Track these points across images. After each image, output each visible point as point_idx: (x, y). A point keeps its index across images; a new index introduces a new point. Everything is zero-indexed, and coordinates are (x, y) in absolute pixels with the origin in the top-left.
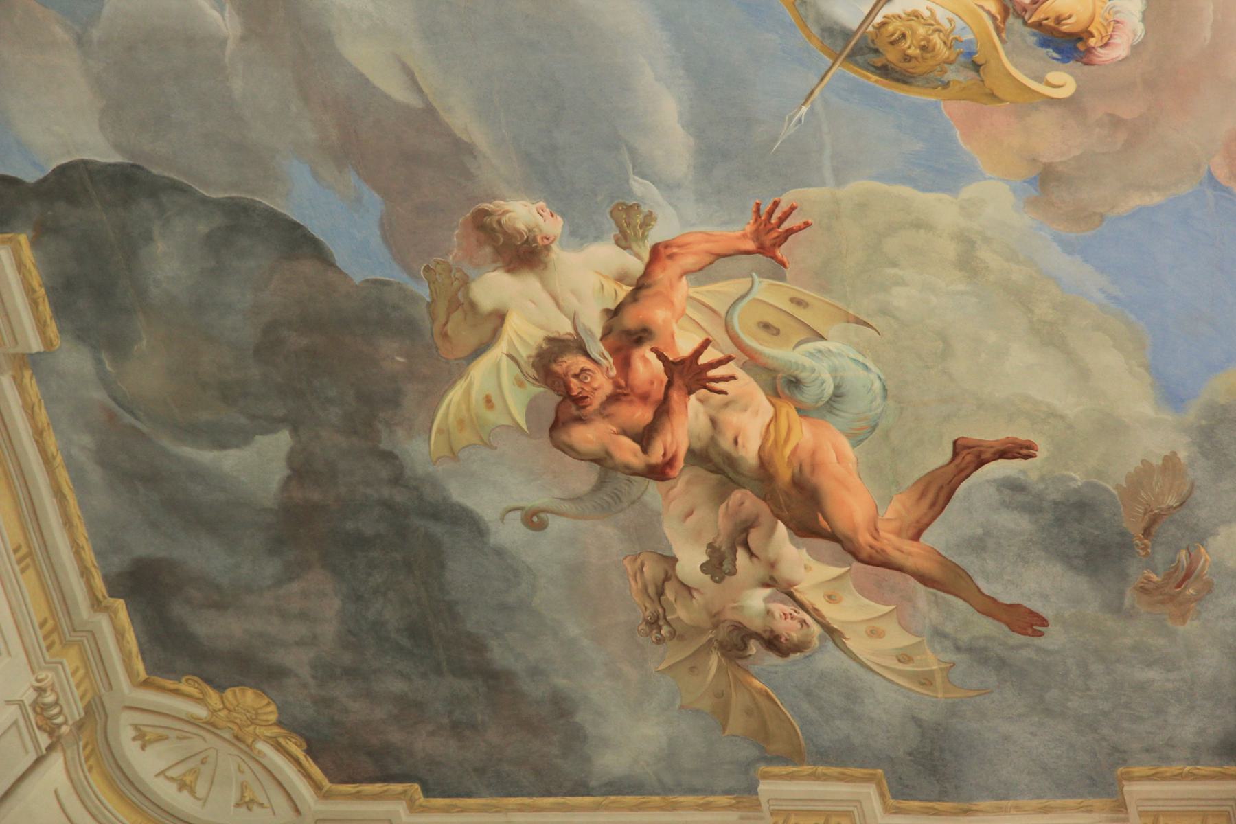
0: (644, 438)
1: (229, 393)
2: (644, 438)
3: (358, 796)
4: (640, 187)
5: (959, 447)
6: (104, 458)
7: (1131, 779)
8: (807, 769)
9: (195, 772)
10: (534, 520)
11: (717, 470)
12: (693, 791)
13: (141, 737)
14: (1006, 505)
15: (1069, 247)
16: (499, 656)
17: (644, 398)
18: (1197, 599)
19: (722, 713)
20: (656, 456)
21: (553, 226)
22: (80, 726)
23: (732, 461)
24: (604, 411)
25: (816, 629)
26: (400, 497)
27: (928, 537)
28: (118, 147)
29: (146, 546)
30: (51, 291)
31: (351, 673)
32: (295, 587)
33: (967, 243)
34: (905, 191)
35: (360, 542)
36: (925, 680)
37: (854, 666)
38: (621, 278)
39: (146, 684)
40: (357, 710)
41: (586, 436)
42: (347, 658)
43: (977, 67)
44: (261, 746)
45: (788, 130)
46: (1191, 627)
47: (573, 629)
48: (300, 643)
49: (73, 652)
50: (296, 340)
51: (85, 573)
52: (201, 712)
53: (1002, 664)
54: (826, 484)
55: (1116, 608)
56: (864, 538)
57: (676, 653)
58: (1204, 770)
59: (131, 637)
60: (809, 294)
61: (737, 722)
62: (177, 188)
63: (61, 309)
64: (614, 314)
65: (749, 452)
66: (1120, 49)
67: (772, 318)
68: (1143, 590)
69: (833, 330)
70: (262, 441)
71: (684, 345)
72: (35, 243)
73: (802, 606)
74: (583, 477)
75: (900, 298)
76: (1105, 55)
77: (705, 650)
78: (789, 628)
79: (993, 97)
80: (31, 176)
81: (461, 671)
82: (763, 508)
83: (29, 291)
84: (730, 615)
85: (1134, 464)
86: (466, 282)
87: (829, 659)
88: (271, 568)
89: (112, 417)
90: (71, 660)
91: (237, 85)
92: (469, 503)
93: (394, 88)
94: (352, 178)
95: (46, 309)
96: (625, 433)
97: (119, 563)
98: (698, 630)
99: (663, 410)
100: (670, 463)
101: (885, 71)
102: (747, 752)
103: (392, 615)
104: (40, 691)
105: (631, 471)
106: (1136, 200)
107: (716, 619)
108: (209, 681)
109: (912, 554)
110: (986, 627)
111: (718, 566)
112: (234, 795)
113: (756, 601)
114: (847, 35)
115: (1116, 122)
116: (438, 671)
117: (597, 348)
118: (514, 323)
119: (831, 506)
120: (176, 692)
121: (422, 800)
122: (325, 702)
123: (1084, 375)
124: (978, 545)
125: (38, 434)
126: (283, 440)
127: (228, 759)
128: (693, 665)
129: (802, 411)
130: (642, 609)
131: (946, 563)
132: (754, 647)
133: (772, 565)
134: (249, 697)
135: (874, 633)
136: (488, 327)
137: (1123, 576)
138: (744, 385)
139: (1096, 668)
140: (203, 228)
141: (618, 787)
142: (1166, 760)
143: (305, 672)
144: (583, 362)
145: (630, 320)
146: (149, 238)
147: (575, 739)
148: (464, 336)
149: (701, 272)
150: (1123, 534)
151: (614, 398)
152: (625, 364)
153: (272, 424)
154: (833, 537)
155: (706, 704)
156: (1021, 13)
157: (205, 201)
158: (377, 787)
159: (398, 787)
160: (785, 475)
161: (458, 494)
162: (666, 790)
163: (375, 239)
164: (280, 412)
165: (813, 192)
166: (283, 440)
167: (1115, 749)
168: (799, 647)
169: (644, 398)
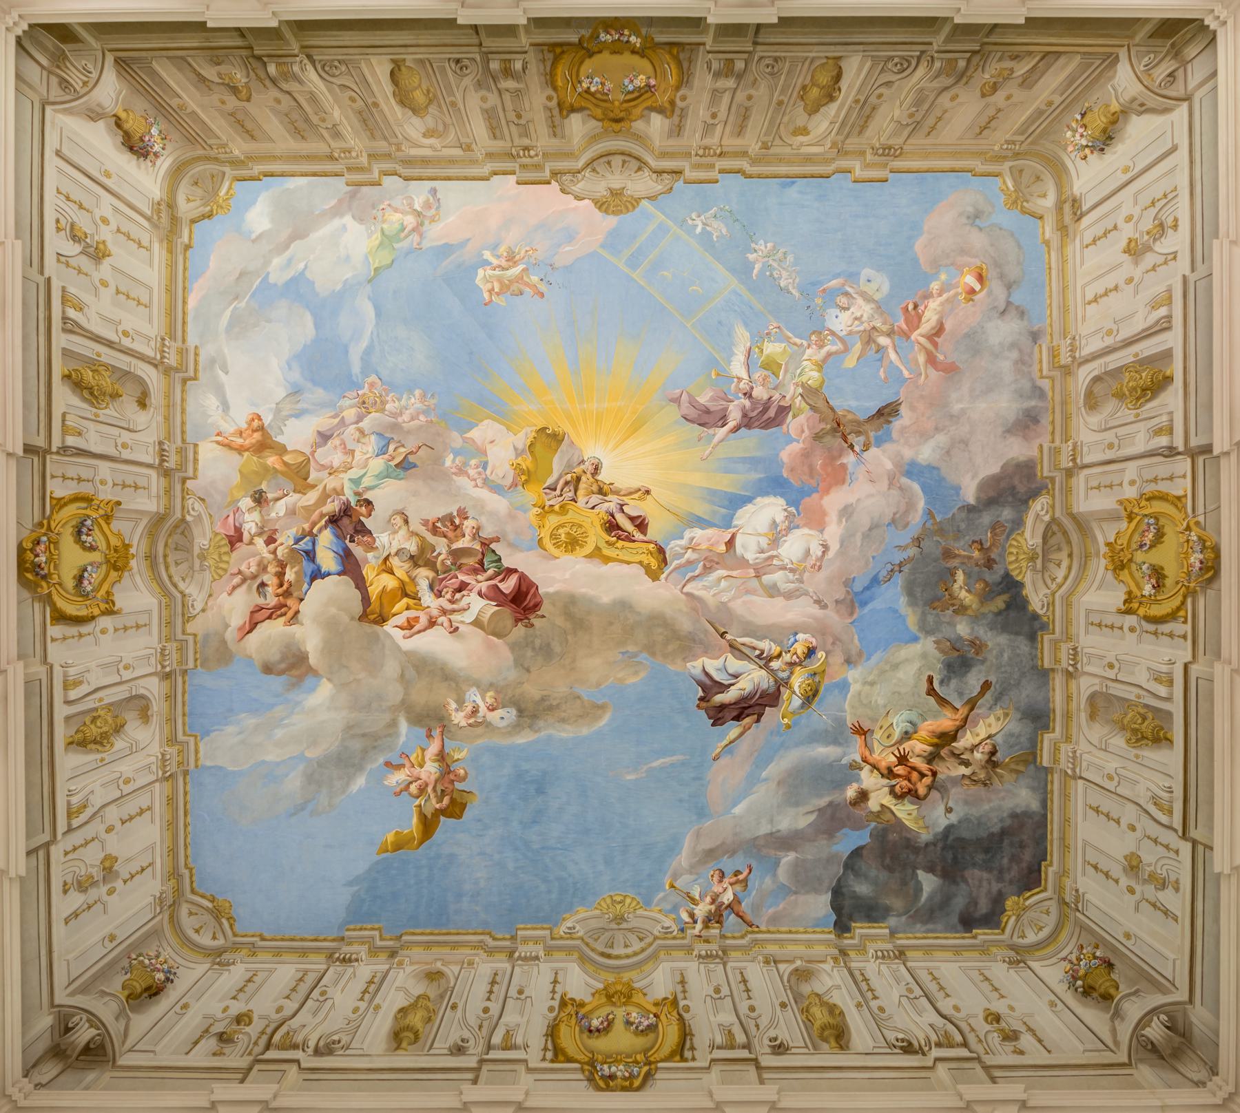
0: (923, 775)
1: (904, 883)
2: (923, 775)
3: (1046, 880)
4: (844, 761)
5: (928, 694)
6: (925, 923)
7: (1043, 665)
8: (1038, 752)
9: (1036, 925)
10: (949, 810)
11: (934, 758)
12: (1046, 785)
13: (1023, 937)
14: (948, 685)
15: (869, 659)
16: (996, 829)
17: (909, 773)
18: (980, 641)
19: (1018, 772)
20: (929, 773)
21: (855, 786)
22: (1017, 953)
23: (931, 754)
24: (914, 784)
25: (988, 741)
26: (940, 845)
27: (958, 706)
28: (827, 892)
29: (955, 919)
30: (869, 922)
31: (1001, 871)
32: (970, 881)
33: (865, 683)
34: (849, 696)
35: (955, 858)
36: (1006, 715)
37: (1002, 732)
38: (872, 772)
39: (1003, 931)
40: (1014, 872)
41: (922, 790)
42: (995, 872)
43: (815, 674)
44: (1027, 903)
45: (829, 721)
46: (990, 644)
47: (986, 807)
48: (990, 884)
49: (991, 949)
50: (888, 861)
51: (963, 938)
52: (1013, 918)
53: (1001, 693)
54: (940, 730)
55: (983, 662)
56: (958, 723)
57: (996, 780)
58: (1040, 646)
59: (986, 931)
60: (879, 724)
61: (1021, 768)
62: (839, 880)
63: (876, 921)
64: (883, 776)
65: (929, 749)
66: (814, 641)
67: (886, 735)
68: (977, 654)
69: (890, 720)
70: (920, 878)
71: (894, 759)
72: (855, 922)
73: (980, 744)
74: (935, 794)
75: (881, 701)
76: (814, 643)
77: (996, 773)
78: (988, 748)
79: (824, 671)
80: (834, 917)
81: (1001, 841)
82: (947, 748)
83: (869, 927)
84: (983, 763)
85: (936, 652)
86: (872, 812)
87: (999, 739)
88: (963, 886)
89: (910, 917)
90: (994, 950)
91: (809, 857)
92: (943, 827)
93: (812, 817)
94: (838, 834)
95: (876, 925)
96: (921, 780)
97: (960, 927)
98: (988, 773)
99: (914, 769)
100: (931, 770)
101: (814, 696)
102: (1032, 767)
103: (980, 857)
104: (1004, 961)
105: (934, 781)
106: (856, 641)
107: (983, 767)
108: (1003, 913)
109: (963, 712)
110: (988, 696)
111: (966, 764)
112: (1045, 916)
113: (978, 755)
114: (803, 703)
115: (833, 643)
116: (1001, 848)
117: (893, 782)
118: (885, 802)
119: (947, 730)
120: (1006, 923)
121: (1048, 862)
122: (1011, 882)
123: (907, 660)
124: (961, 694)
125: (915, 938)
126: (920, 873)
127: (1030, 914)
128: (1000, 777)
129: (916, 732)
130: (980, 787)
131: (967, 703)
132: (994, 759)
133: (966, 749)
134: (1009, 903)
135: (990, 725)
136: (887, 810)
137: (972, 658)
138: (907, 746)
139: (1003, 669)
140: (852, 877)
141: (1044, 804)
142: (1036, 656)
143: (1000, 885)
144: (898, 787)
145: (885, 772)
146: (855, 892)
147: (1027, 814)
148: (888, 816)
149: (871, 751)
150: (958, 657)
151: (909, 781)
152: (899, 776)
153: (915, 875)
154: (957, 731)
155: (1014, 776)
156: (801, 661)
157: (844, 874)
158: (1043, 874)
159: (1043, 868)
160: (936, 740)
161: (940, 829)
162: (1045, 792)
163: (857, 833)
164: (910, 871)
165: (848, 719)
166: (920, 873)
167: (1032, 668)
168: (994, 747)
169: (909, 773)
